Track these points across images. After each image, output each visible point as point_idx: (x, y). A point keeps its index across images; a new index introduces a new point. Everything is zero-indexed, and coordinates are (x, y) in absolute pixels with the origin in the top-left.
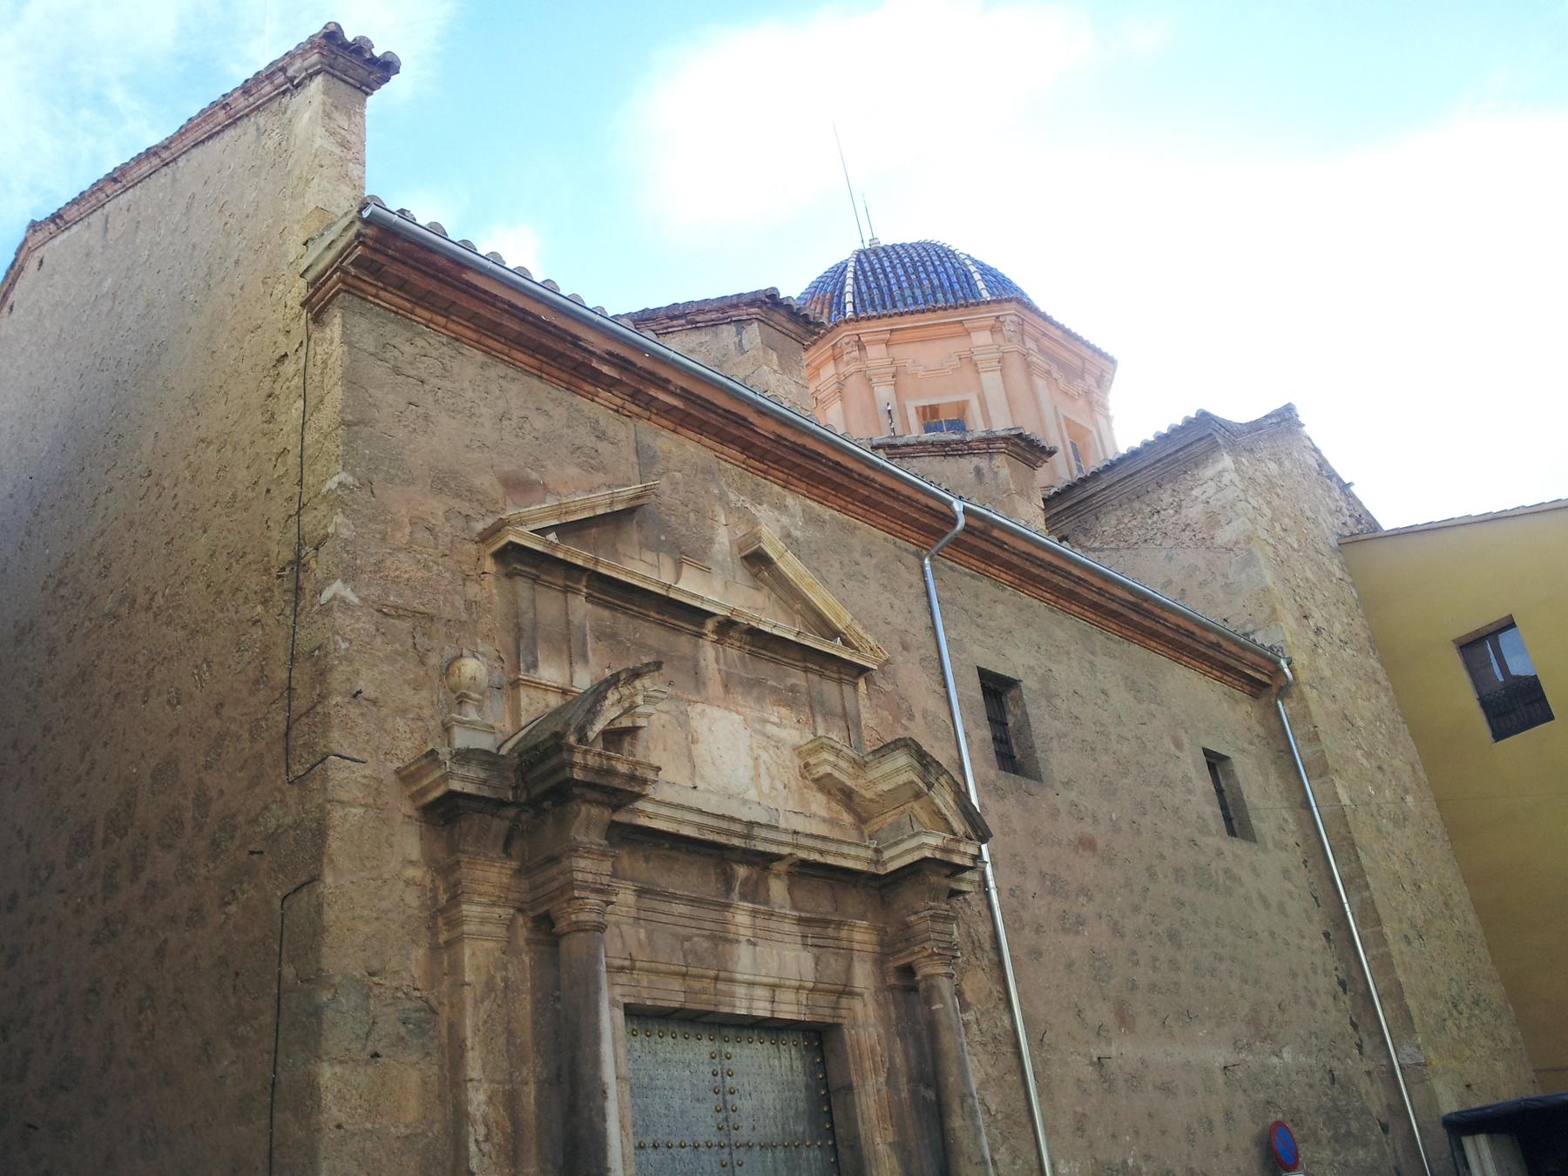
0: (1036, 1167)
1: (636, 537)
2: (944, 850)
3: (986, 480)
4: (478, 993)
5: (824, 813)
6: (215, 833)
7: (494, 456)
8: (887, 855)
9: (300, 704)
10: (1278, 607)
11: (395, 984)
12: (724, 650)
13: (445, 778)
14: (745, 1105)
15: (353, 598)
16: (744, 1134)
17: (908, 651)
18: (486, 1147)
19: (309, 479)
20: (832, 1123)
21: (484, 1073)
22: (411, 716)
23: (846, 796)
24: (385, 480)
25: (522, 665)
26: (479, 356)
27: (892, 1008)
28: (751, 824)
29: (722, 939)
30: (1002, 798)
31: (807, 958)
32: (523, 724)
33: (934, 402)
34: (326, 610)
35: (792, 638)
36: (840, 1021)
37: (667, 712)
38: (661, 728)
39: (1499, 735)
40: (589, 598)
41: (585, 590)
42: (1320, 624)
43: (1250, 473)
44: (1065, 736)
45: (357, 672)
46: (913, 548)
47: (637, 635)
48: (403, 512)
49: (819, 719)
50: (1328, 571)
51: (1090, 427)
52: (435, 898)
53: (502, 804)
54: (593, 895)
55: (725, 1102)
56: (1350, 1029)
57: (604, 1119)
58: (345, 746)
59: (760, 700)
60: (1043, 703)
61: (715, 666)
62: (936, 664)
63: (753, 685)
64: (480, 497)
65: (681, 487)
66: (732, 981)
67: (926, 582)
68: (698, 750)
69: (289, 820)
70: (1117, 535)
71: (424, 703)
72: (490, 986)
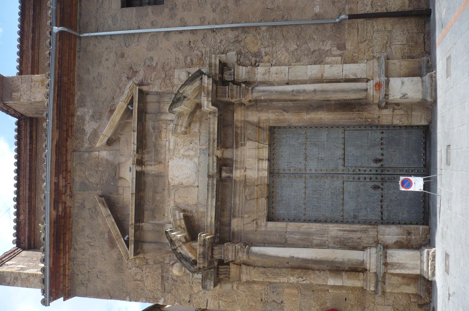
1: (116, 196)
5: (198, 125)
11: (264, 294)
12: (147, 161)
17: (124, 54)
18: (304, 278)
26: (72, 251)
28: (209, 176)
29: (245, 182)
31: (249, 144)
35: (136, 133)
36: (268, 128)
37: (174, 195)
38: (180, 198)
55: (292, 174)
61: (153, 167)
72: (264, 273)
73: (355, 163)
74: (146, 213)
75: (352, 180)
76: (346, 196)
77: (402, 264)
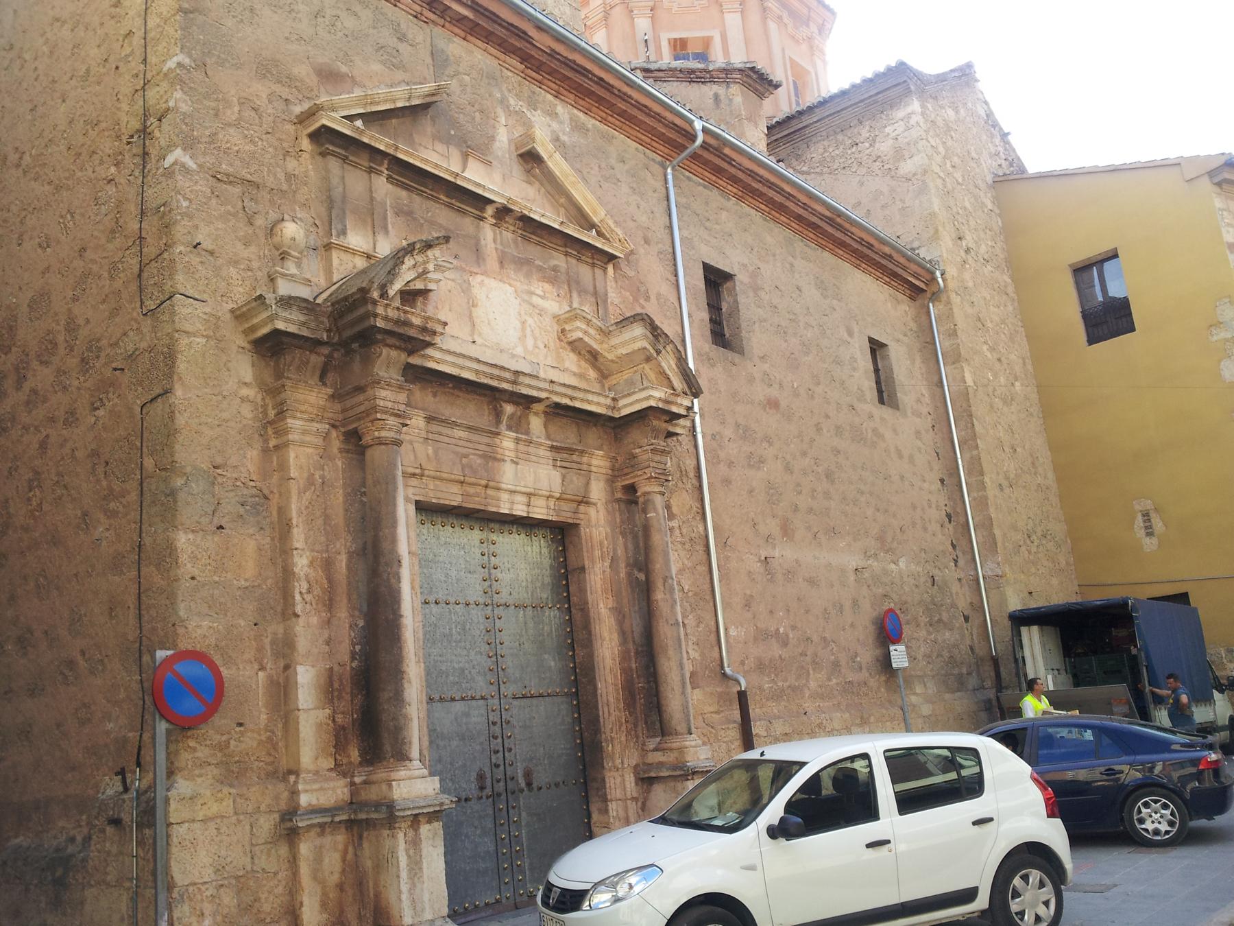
0: (714, 629)
1: (429, 129)
2: (667, 402)
3: (722, 105)
4: (302, 486)
5: (575, 369)
6: (83, 354)
7: (310, 48)
8: (621, 403)
9: (150, 251)
10: (940, 228)
11: (235, 475)
12: (501, 233)
13: (272, 318)
14: (505, 577)
15: (191, 164)
16: (504, 597)
17: (649, 245)
18: (308, 597)
19: (152, 59)
20: (568, 592)
21: (306, 543)
22: (242, 267)
23: (593, 357)
24: (217, 63)
25: (334, 232)
27: (618, 514)
28: (517, 373)
29: (492, 457)
30: (713, 366)
31: (556, 476)
32: (335, 280)
33: (683, 35)
34: (169, 173)
35: (556, 226)
36: (578, 522)
39: (1092, 340)
40: (389, 178)
41: (386, 172)
42: (970, 245)
43: (933, 116)
44: (765, 320)
45: (197, 227)
46: (659, 159)
47: (430, 214)
48: (233, 92)
49: (575, 295)
50: (983, 203)
51: (809, 68)
52: (265, 413)
53: (319, 343)
54: (392, 418)
55: (490, 574)
56: (950, 548)
57: (399, 580)
58: (188, 287)
59: (528, 275)
60: (751, 294)
61: (493, 245)
62: (670, 257)
63: (523, 263)
64: (298, 84)
65: (469, 89)
66: (499, 489)
67: (667, 188)
68: (478, 313)
69: (144, 345)
70: (822, 162)
71: (252, 256)
72: (310, 481)
73: (520, 724)
74: (403, 194)
75: (491, 718)
76: (459, 707)
77: (421, 869)
